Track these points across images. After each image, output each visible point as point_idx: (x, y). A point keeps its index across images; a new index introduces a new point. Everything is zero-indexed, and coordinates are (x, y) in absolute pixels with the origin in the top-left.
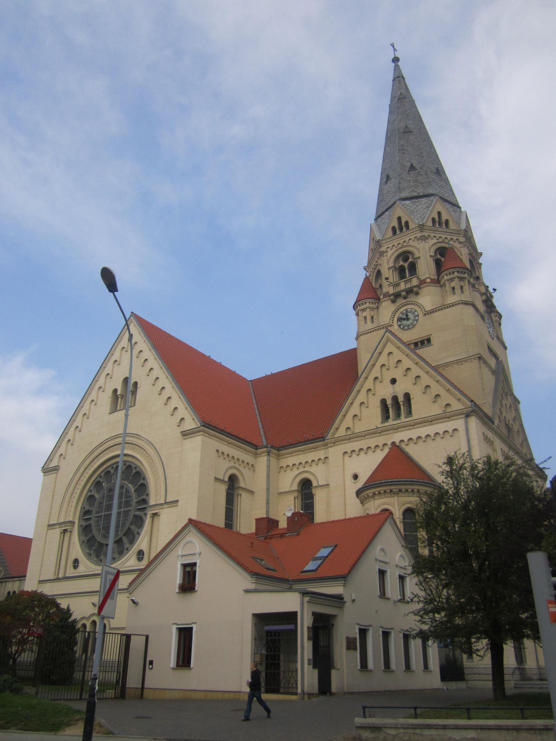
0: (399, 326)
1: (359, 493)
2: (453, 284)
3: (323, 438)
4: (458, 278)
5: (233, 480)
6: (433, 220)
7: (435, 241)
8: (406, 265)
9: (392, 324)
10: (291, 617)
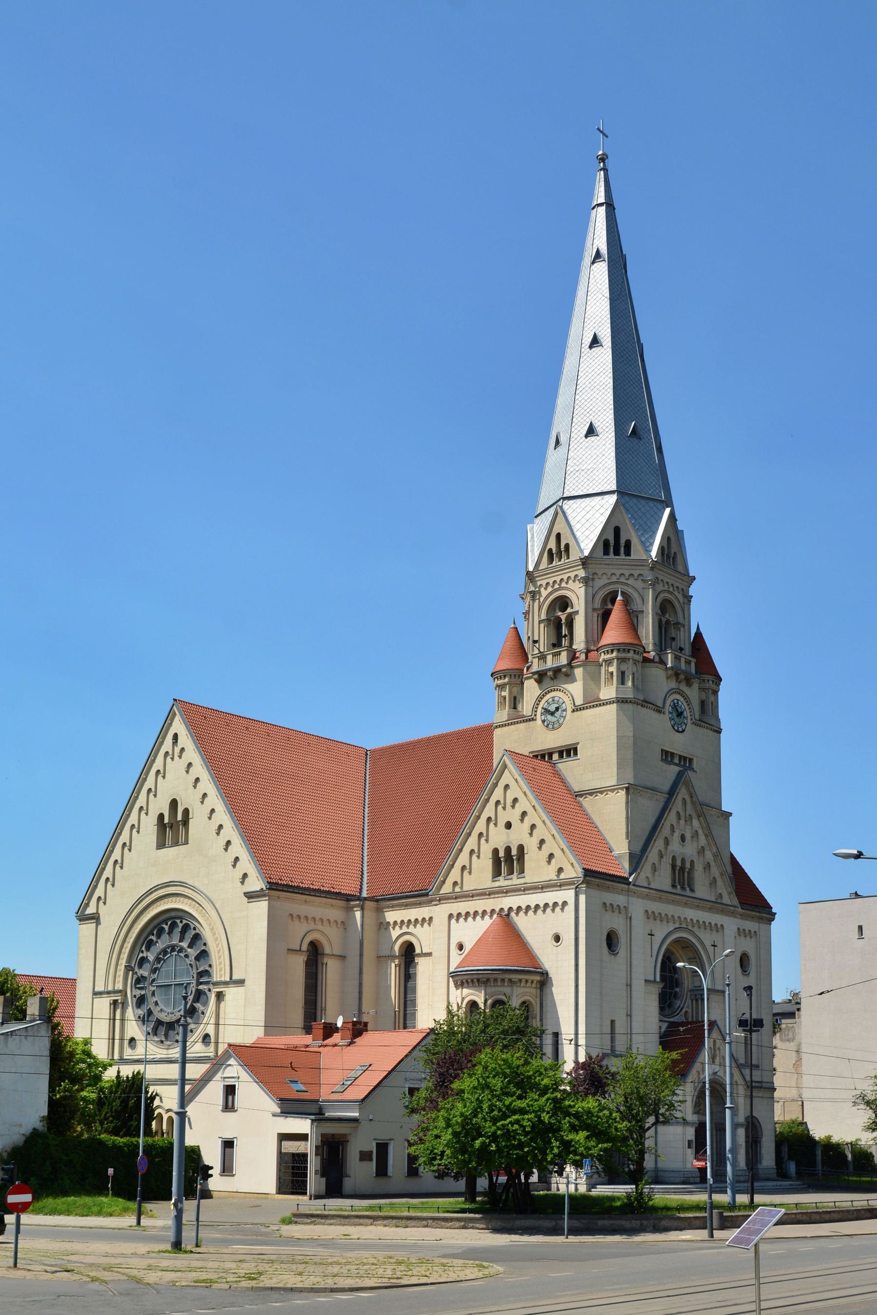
0: (543, 721)
7: (604, 581)
8: (563, 617)
10: (303, 1137)
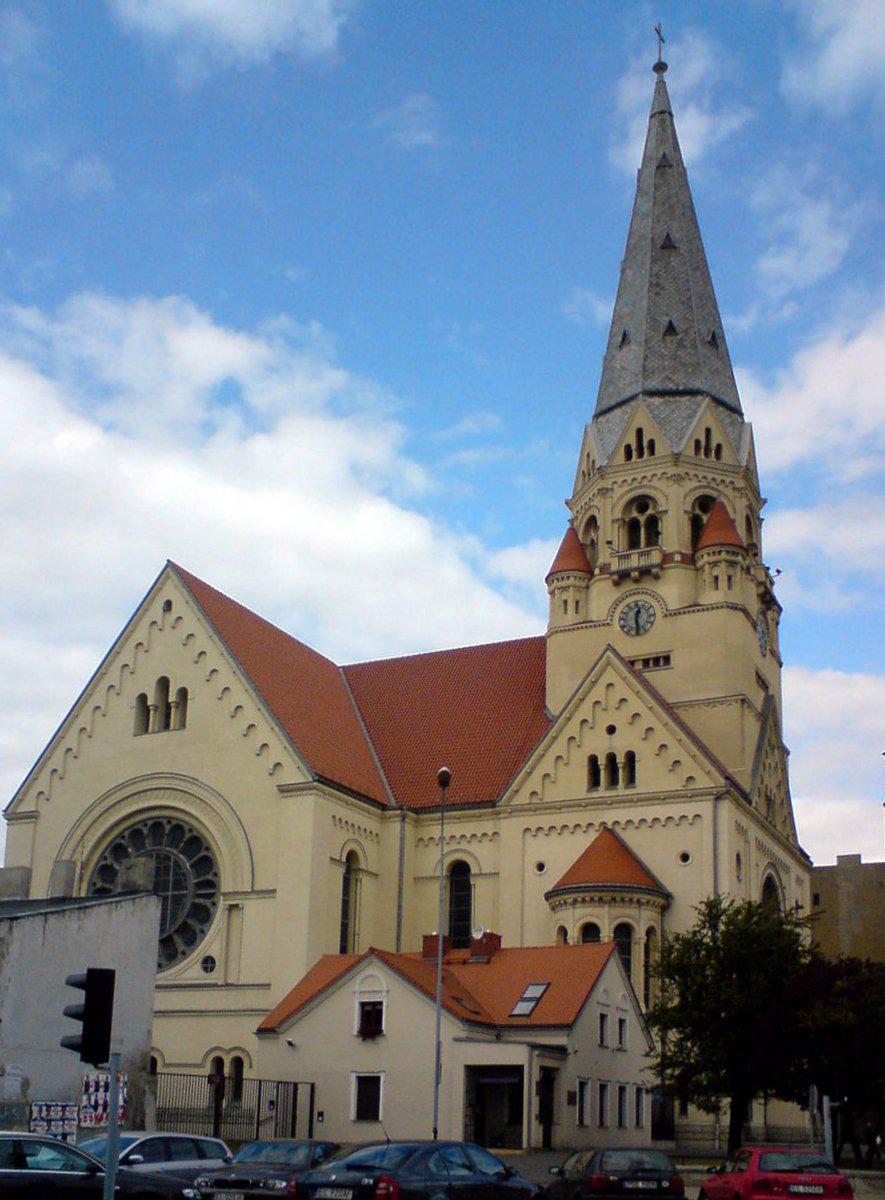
0: (623, 627)
1: (548, 896)
2: (716, 572)
3: (493, 804)
4: (726, 561)
5: (352, 856)
6: (697, 443)
7: (694, 484)
8: (642, 519)
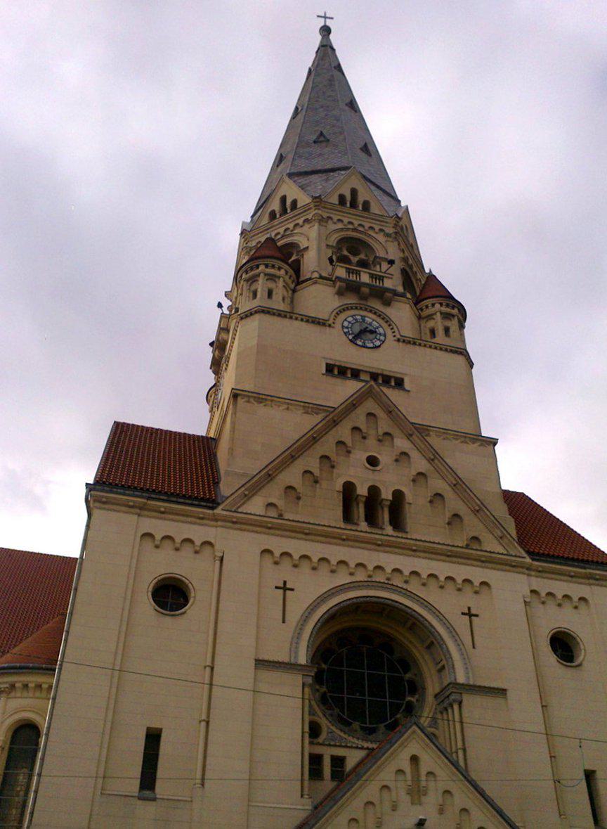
9: (332, 325)
